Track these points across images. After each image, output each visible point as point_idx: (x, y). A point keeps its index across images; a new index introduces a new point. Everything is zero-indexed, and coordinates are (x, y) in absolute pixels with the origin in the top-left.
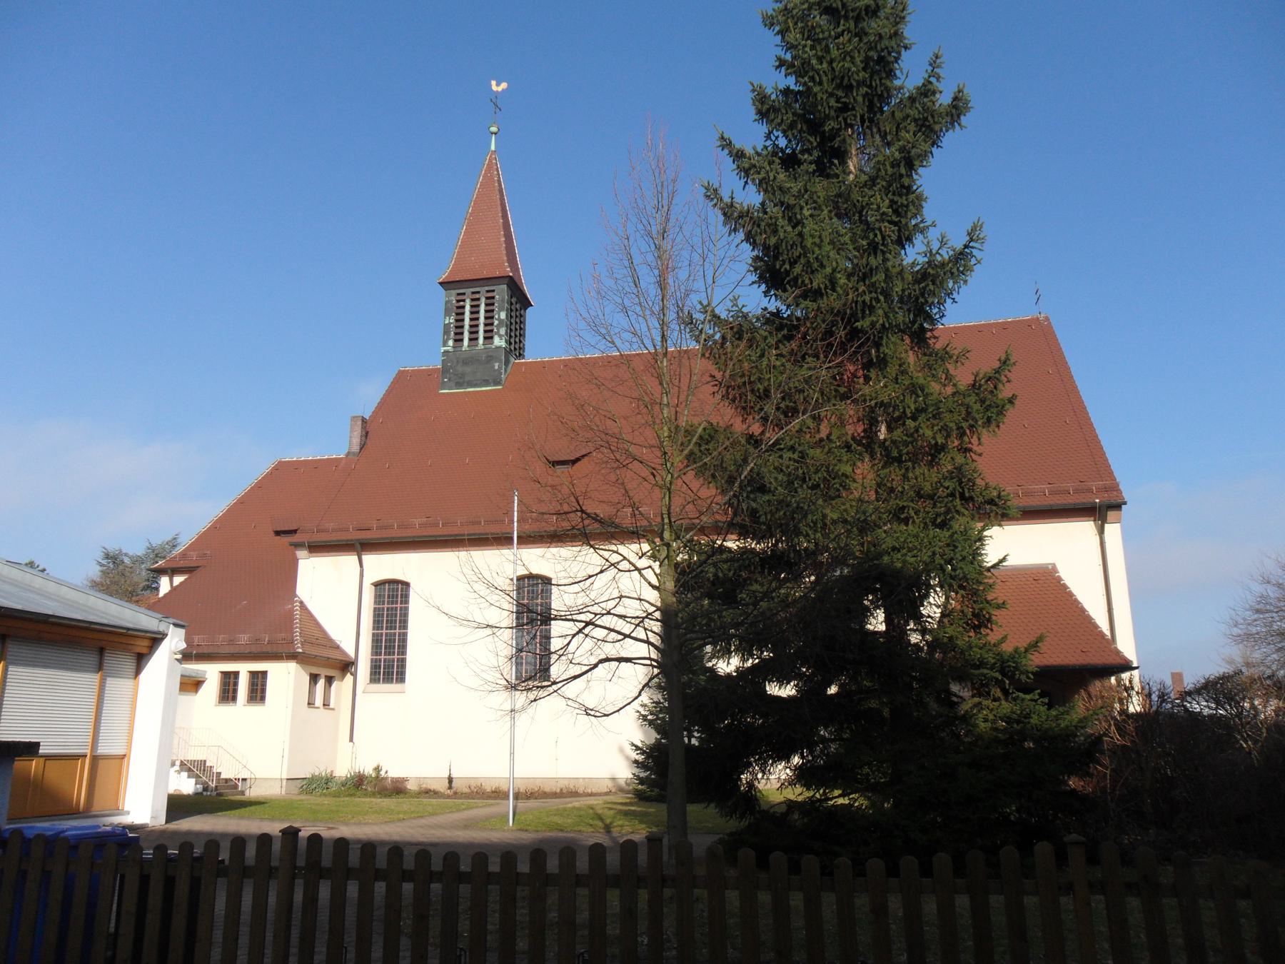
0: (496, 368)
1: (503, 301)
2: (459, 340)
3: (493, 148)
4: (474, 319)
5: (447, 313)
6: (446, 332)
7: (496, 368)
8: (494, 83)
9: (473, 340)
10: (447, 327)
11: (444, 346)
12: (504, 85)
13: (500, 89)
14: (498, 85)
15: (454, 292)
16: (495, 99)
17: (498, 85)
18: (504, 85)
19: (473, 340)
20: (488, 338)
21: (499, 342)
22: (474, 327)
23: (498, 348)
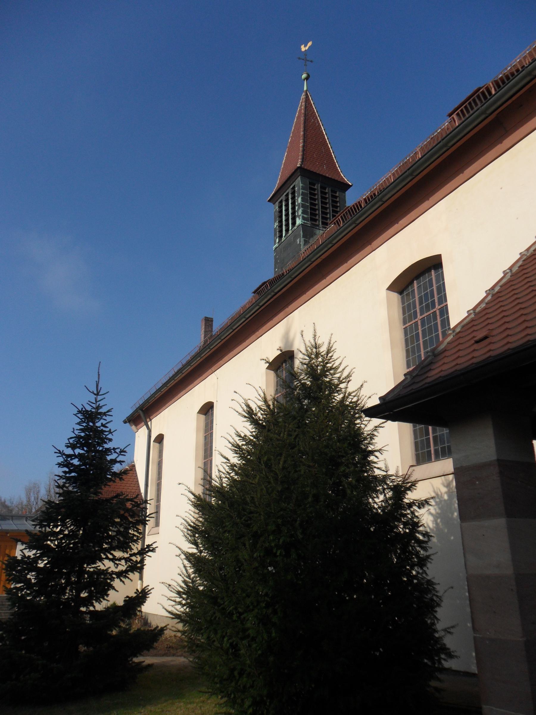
0: (298, 243)
1: (299, 190)
2: (281, 237)
3: (305, 89)
4: (287, 215)
6: (275, 235)
7: (298, 243)
8: (302, 47)
9: (287, 230)
10: (275, 229)
11: (275, 244)
12: (310, 44)
13: (307, 48)
14: (305, 46)
15: (277, 203)
16: (305, 58)
17: (305, 46)
18: (310, 44)
19: (287, 230)
20: (294, 223)
21: (299, 221)
22: (287, 220)
23: (299, 225)
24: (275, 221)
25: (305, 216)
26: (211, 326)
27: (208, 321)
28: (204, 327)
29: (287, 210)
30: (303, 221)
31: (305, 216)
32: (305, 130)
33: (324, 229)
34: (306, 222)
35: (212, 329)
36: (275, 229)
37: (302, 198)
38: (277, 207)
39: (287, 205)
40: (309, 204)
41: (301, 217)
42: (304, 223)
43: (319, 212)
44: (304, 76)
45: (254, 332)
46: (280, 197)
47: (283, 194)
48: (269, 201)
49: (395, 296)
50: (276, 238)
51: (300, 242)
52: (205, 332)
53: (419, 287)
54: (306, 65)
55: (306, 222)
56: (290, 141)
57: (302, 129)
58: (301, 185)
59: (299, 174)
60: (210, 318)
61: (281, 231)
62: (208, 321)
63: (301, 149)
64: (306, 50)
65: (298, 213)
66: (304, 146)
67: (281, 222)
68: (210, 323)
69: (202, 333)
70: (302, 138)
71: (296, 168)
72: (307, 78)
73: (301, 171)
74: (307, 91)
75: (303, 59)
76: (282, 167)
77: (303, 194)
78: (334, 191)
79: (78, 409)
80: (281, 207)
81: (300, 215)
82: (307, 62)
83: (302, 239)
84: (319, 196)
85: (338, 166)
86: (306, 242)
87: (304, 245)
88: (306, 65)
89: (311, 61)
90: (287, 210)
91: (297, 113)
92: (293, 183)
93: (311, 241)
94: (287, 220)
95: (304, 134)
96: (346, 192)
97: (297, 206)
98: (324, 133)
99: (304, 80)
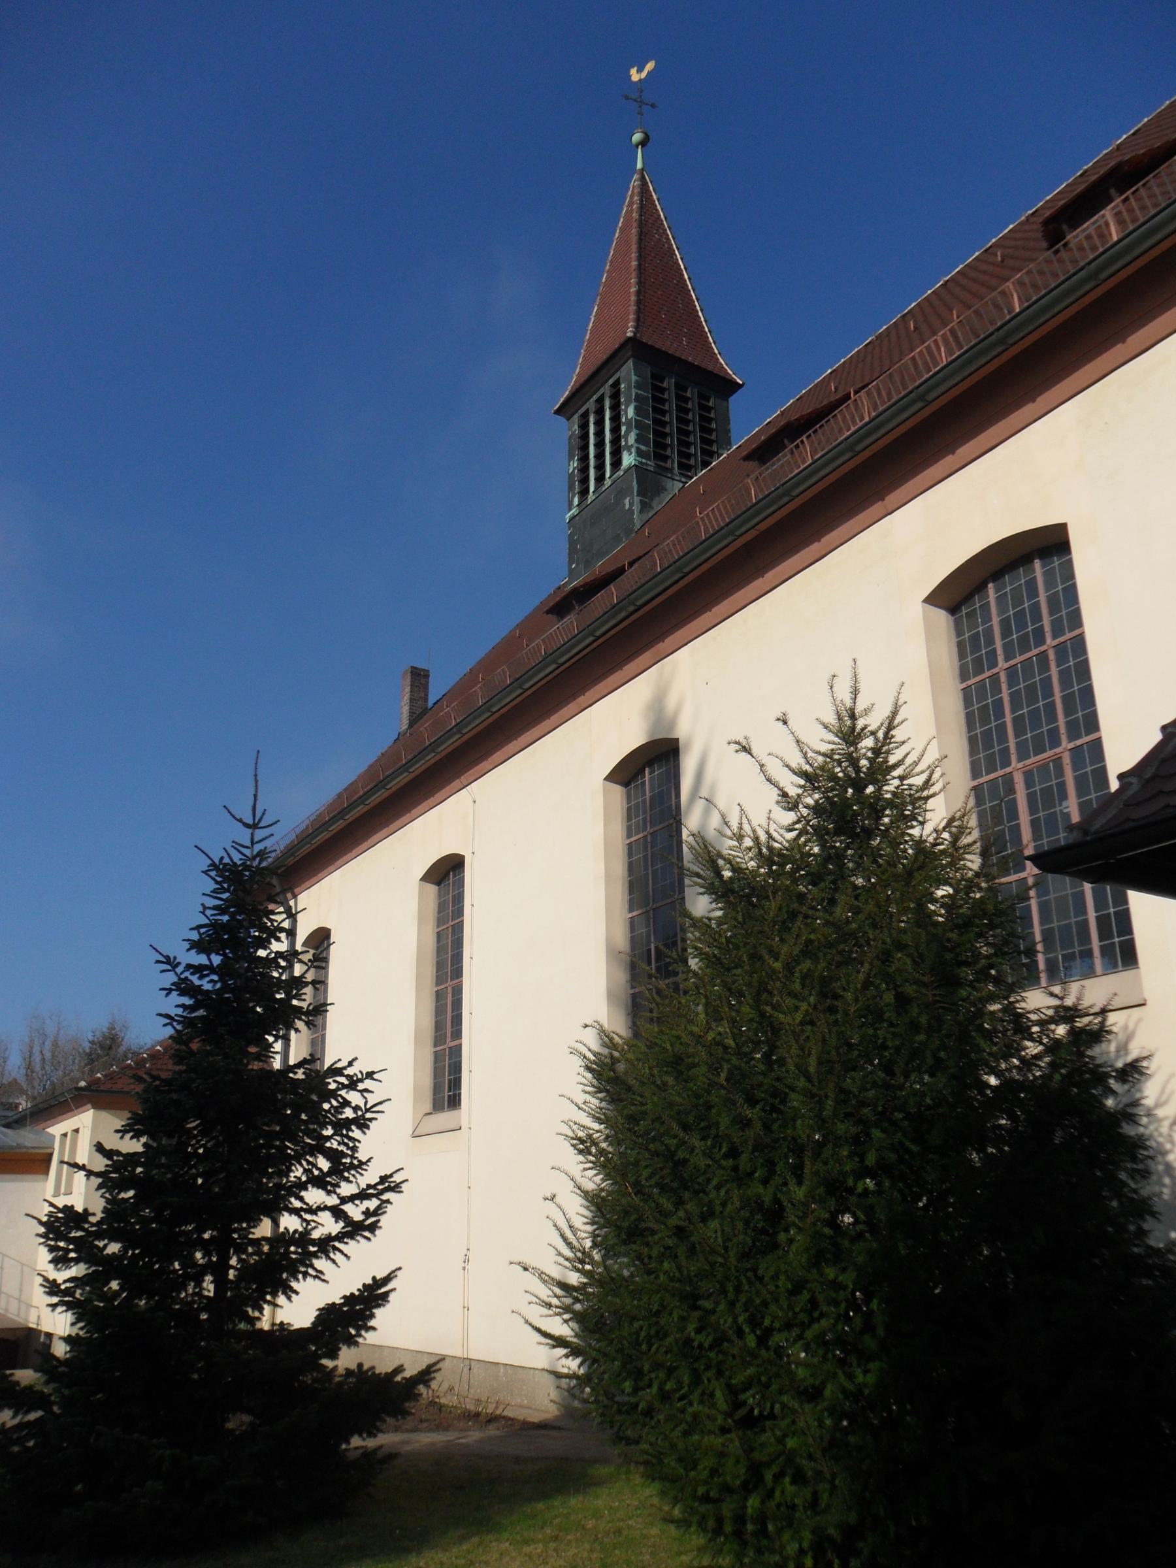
0: (627, 506)
1: (629, 388)
2: (584, 492)
3: (639, 165)
4: (600, 445)
5: (571, 458)
6: (571, 487)
7: (627, 506)
8: (633, 71)
9: (600, 479)
10: (571, 475)
11: (570, 510)
12: (650, 66)
13: (644, 75)
14: (640, 71)
15: (576, 417)
16: (639, 96)
17: (640, 71)
18: (650, 66)
19: (600, 479)
20: (617, 464)
21: (628, 460)
22: (600, 456)
23: (630, 468)
24: (571, 458)
25: (643, 448)
26: (425, 687)
27: (419, 678)
28: (408, 689)
29: (600, 433)
30: (640, 459)
31: (643, 448)
32: (641, 258)
33: (683, 480)
34: (644, 461)
35: (427, 695)
36: (571, 475)
37: (636, 408)
38: (576, 427)
39: (600, 423)
40: (651, 423)
41: (633, 450)
42: (641, 463)
43: (673, 440)
44: (637, 137)
45: (573, 697)
46: (583, 405)
47: (591, 397)
48: (558, 412)
49: (941, 617)
50: (573, 496)
51: (631, 504)
52: (412, 700)
53: (1000, 600)
54: (641, 113)
55: (644, 461)
56: (604, 280)
57: (634, 255)
58: (634, 378)
59: (630, 353)
60: (424, 670)
61: (585, 481)
62: (419, 678)
63: (633, 298)
64: (640, 80)
65: (626, 441)
66: (638, 293)
67: (584, 459)
68: (423, 681)
69: (403, 704)
70: (634, 274)
71: (622, 340)
72: (643, 143)
73: (635, 348)
74: (642, 170)
75: (635, 100)
76: (587, 337)
77: (638, 398)
78: (703, 397)
79: (211, 860)
80: (584, 426)
81: (632, 446)
82: (644, 106)
83: (637, 499)
84: (671, 406)
85: (711, 341)
86: (644, 506)
87: (641, 511)
88: (641, 113)
89: (653, 106)
90: (600, 433)
91: (622, 220)
92: (617, 371)
93: (654, 504)
94: (600, 456)
95: (640, 266)
96: (732, 399)
97: (624, 424)
98: (682, 267)
99: (637, 147)
